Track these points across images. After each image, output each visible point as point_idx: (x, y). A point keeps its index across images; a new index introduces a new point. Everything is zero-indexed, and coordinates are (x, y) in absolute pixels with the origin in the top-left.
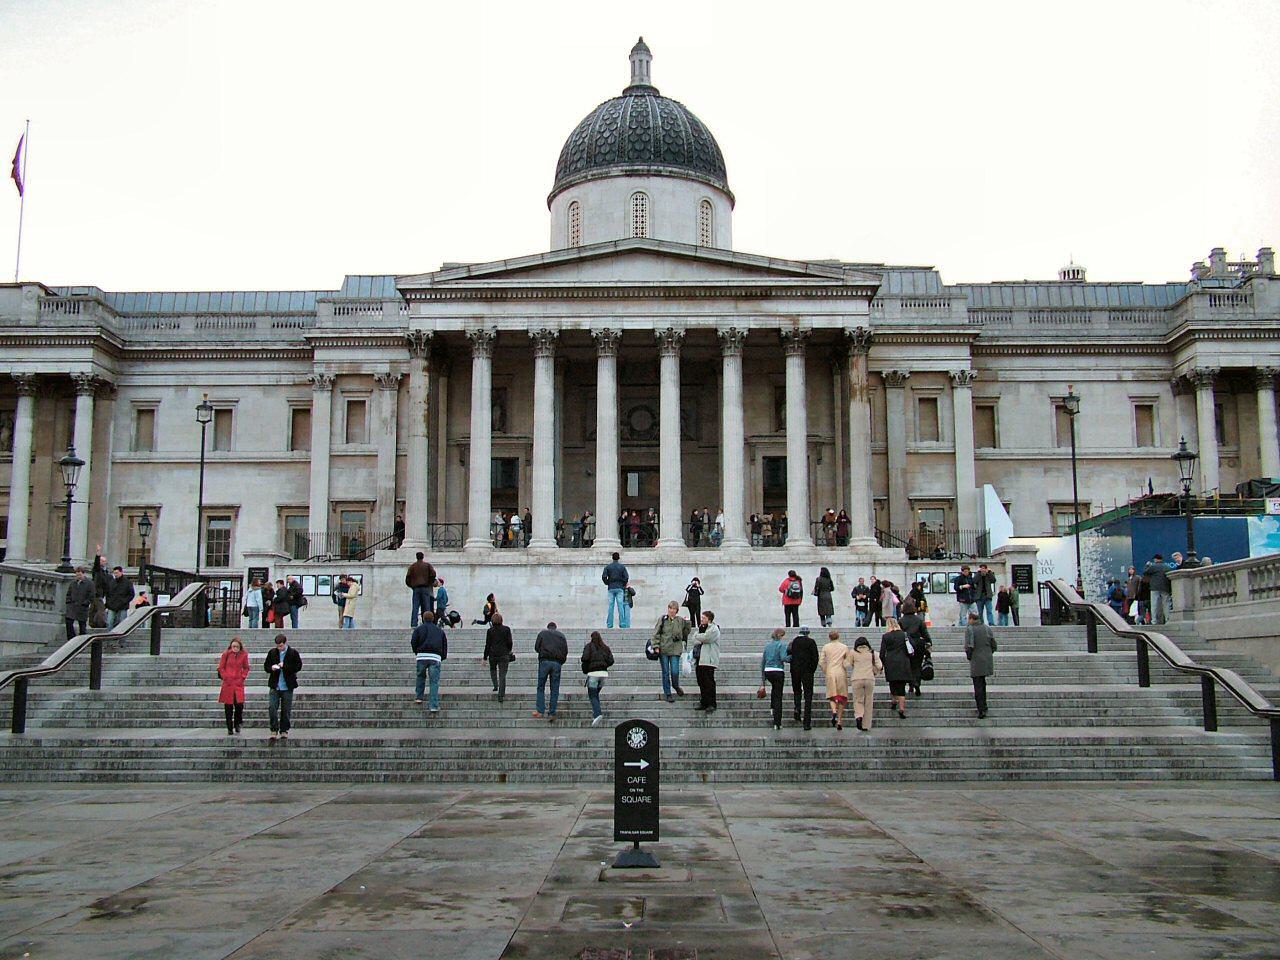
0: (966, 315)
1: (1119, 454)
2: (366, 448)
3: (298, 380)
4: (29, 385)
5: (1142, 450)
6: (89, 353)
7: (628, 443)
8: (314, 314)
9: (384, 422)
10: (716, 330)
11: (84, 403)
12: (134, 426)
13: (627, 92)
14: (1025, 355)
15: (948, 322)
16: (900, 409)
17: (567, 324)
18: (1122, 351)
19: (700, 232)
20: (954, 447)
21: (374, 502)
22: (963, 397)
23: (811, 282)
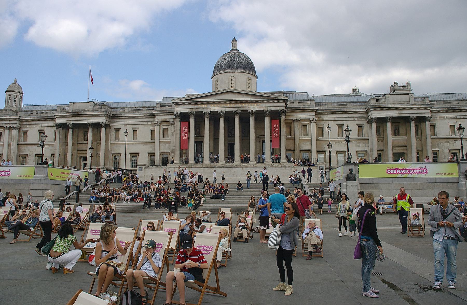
0: (314, 104)
1: (354, 138)
2: (168, 139)
3: (152, 123)
4: (91, 126)
5: (360, 137)
6: (104, 118)
7: (231, 137)
8: (155, 107)
9: (172, 133)
10: (248, 111)
11: (103, 129)
12: (115, 134)
14: (330, 114)
15: (310, 106)
17: (212, 110)
18: (355, 113)
19: (247, 85)
21: (170, 152)
22: (314, 125)
23: (270, 98)
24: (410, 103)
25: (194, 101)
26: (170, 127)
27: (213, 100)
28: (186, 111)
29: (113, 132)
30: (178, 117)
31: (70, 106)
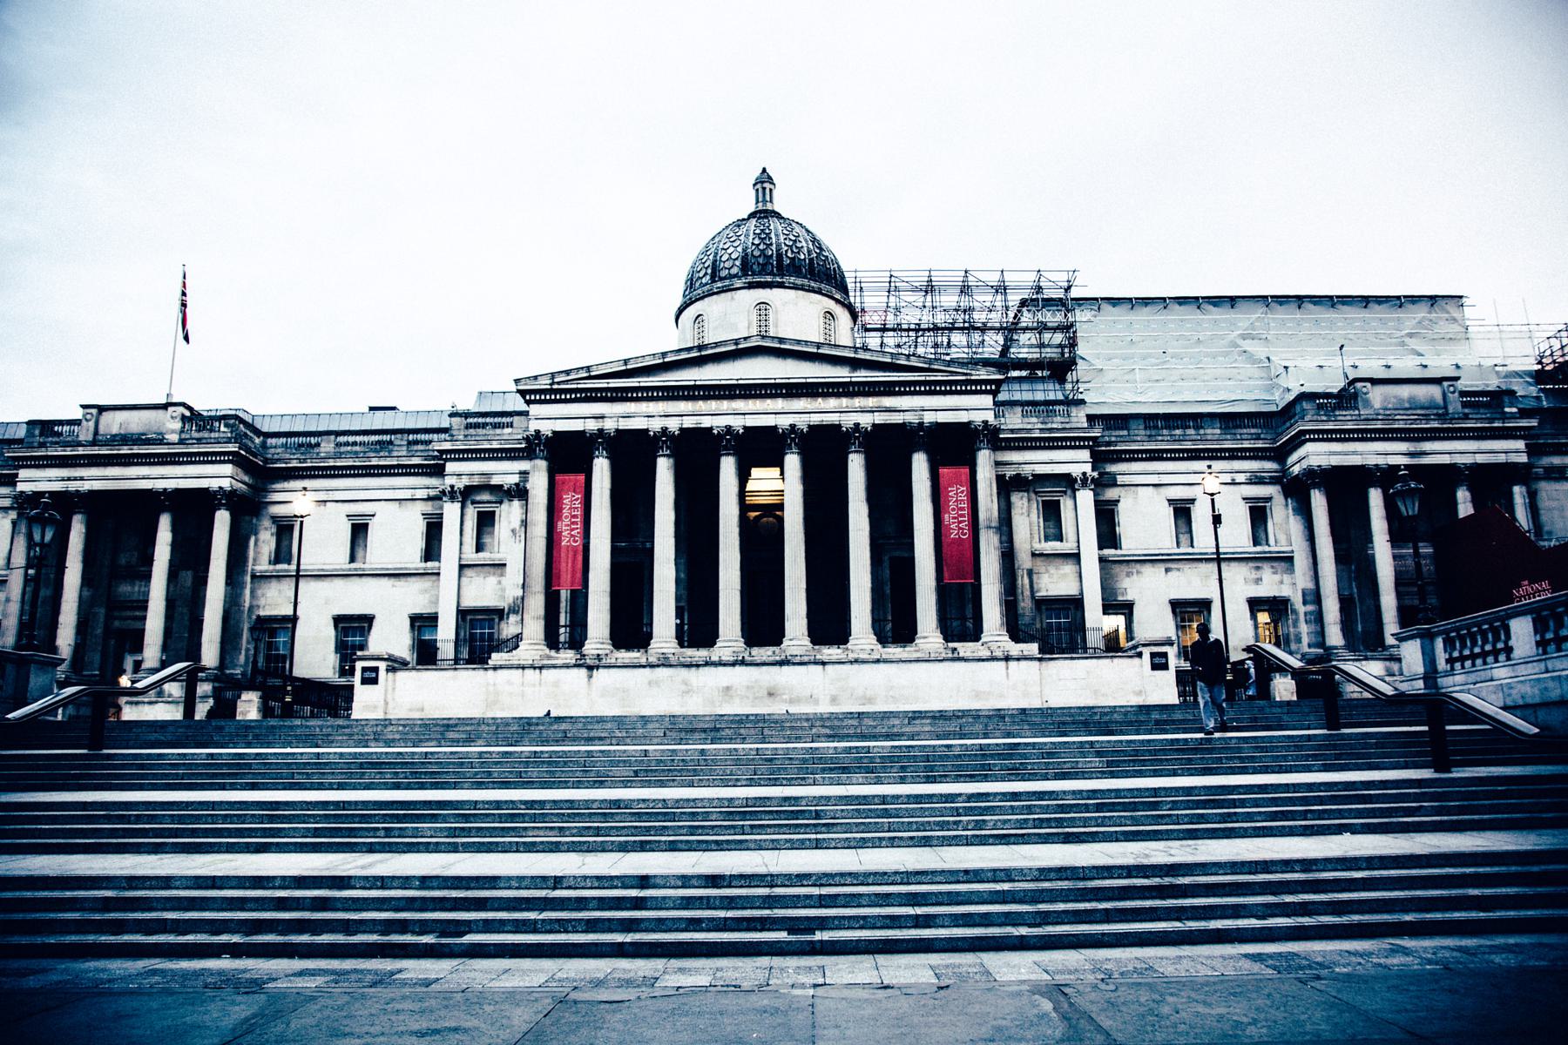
0: (1085, 419)
3: (432, 493)
5: (1259, 549)
6: (228, 469)
11: (222, 519)
13: (752, 215)
15: (1068, 426)
16: (1024, 511)
17: (689, 423)
18: (1234, 455)
20: (1079, 546)
22: (1086, 498)
24: (1447, 414)
25: (610, 385)
26: (503, 506)
27: (692, 383)
28: (576, 426)
29: (266, 529)
30: (543, 451)
31: (84, 423)
